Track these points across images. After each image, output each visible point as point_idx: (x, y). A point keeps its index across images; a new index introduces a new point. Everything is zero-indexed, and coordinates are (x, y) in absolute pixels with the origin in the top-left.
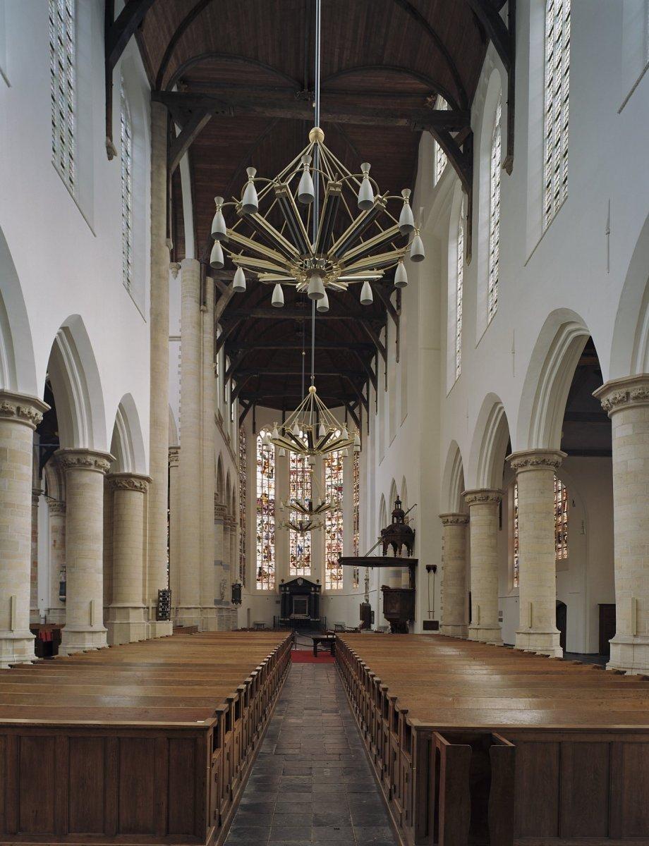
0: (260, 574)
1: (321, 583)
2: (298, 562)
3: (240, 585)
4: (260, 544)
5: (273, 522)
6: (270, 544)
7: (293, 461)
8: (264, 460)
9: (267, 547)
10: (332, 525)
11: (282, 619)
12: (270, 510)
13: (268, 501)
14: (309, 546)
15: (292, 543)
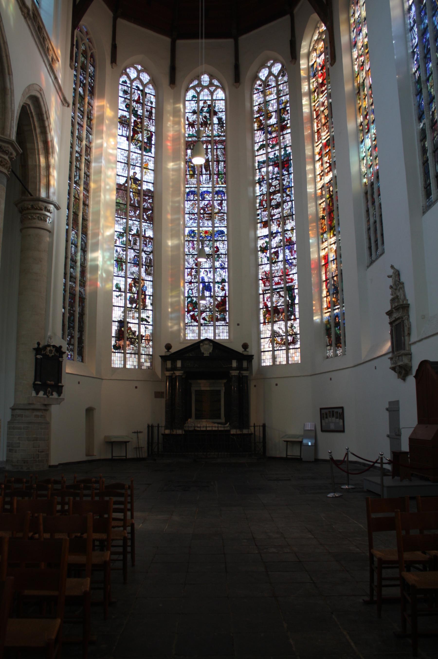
0: (120, 335)
1: (252, 351)
2: (203, 312)
3: (59, 349)
4: (123, 274)
5: (150, 233)
6: (143, 275)
7: (191, 125)
8: (133, 119)
9: (137, 281)
10: (272, 235)
11: (167, 432)
12: (146, 210)
13: (138, 193)
14: (223, 281)
15: (190, 274)
